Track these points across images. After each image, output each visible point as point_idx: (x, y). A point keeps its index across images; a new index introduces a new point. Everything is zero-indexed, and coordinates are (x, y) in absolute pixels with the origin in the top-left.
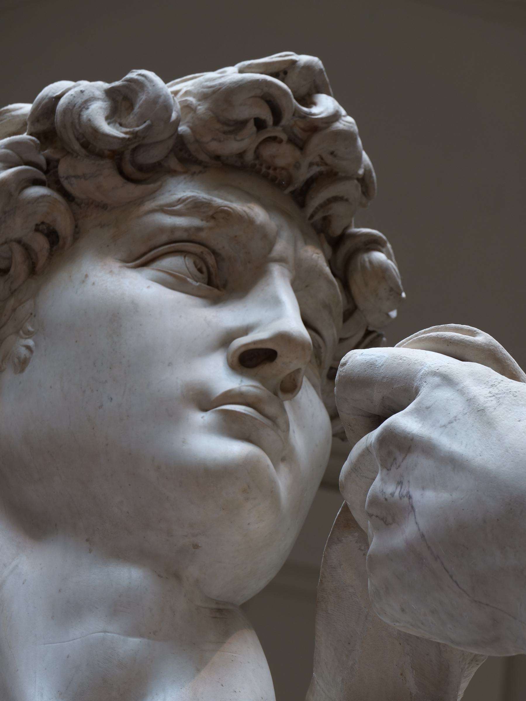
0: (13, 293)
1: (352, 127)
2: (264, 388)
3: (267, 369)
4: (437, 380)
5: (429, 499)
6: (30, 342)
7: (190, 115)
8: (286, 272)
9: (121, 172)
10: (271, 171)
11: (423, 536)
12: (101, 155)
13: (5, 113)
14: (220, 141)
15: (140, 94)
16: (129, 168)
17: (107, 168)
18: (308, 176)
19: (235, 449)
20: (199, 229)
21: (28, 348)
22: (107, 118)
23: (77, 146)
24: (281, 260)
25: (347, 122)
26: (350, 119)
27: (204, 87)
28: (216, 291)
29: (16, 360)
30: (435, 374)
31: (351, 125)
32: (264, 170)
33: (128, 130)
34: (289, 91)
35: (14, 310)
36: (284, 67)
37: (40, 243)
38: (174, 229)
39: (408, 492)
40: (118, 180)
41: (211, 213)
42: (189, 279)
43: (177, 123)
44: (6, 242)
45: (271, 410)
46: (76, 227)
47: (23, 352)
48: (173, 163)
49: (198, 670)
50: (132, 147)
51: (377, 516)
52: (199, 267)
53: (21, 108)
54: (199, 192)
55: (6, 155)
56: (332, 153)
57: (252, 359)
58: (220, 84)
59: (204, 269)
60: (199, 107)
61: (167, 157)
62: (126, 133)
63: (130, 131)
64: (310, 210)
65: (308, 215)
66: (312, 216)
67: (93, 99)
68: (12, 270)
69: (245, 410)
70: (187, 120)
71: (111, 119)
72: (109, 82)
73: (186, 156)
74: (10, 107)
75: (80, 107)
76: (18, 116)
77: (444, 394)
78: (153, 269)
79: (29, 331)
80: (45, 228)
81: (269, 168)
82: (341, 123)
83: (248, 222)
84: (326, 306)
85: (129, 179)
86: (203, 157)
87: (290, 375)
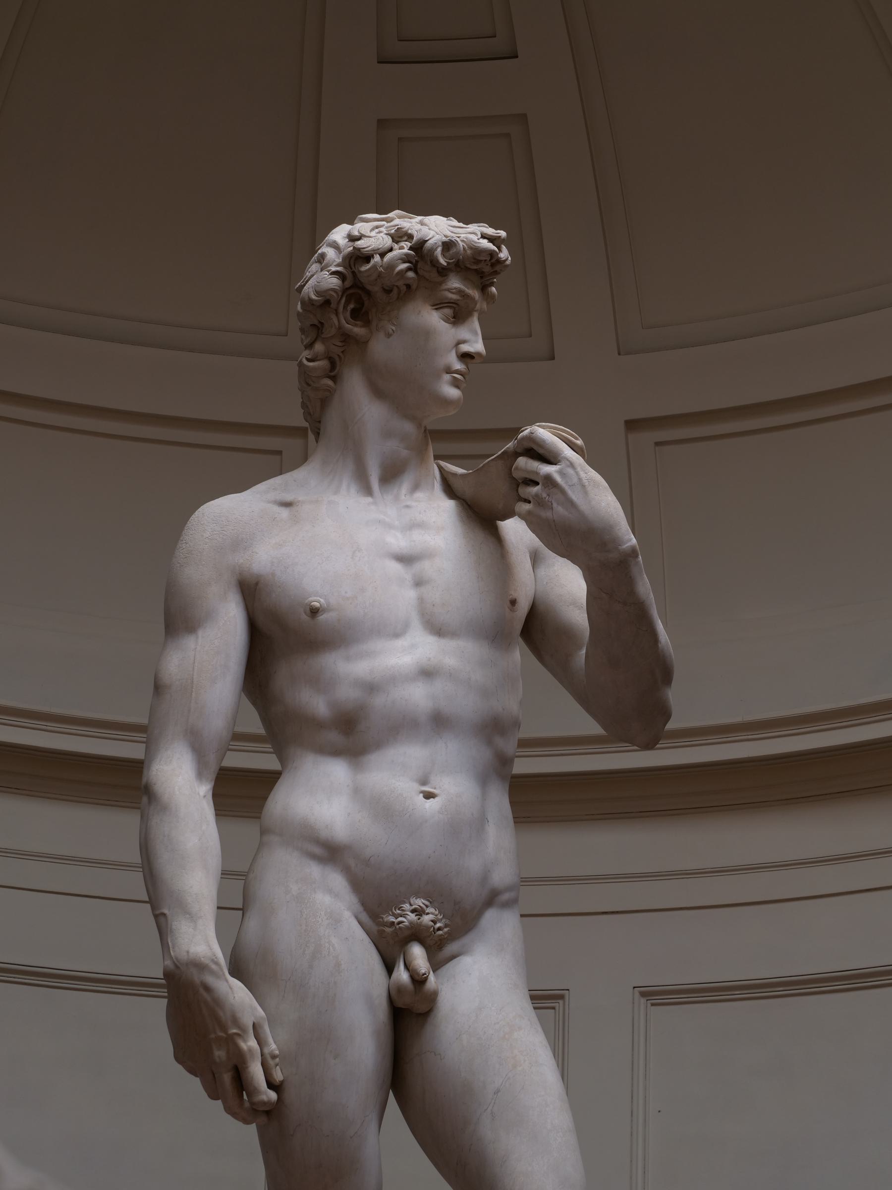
3: (469, 360)
5: (560, 510)
6: (394, 328)
9: (438, 272)
12: (434, 266)
37: (404, 288)
47: (391, 331)
77: (570, 471)
83: (472, 299)
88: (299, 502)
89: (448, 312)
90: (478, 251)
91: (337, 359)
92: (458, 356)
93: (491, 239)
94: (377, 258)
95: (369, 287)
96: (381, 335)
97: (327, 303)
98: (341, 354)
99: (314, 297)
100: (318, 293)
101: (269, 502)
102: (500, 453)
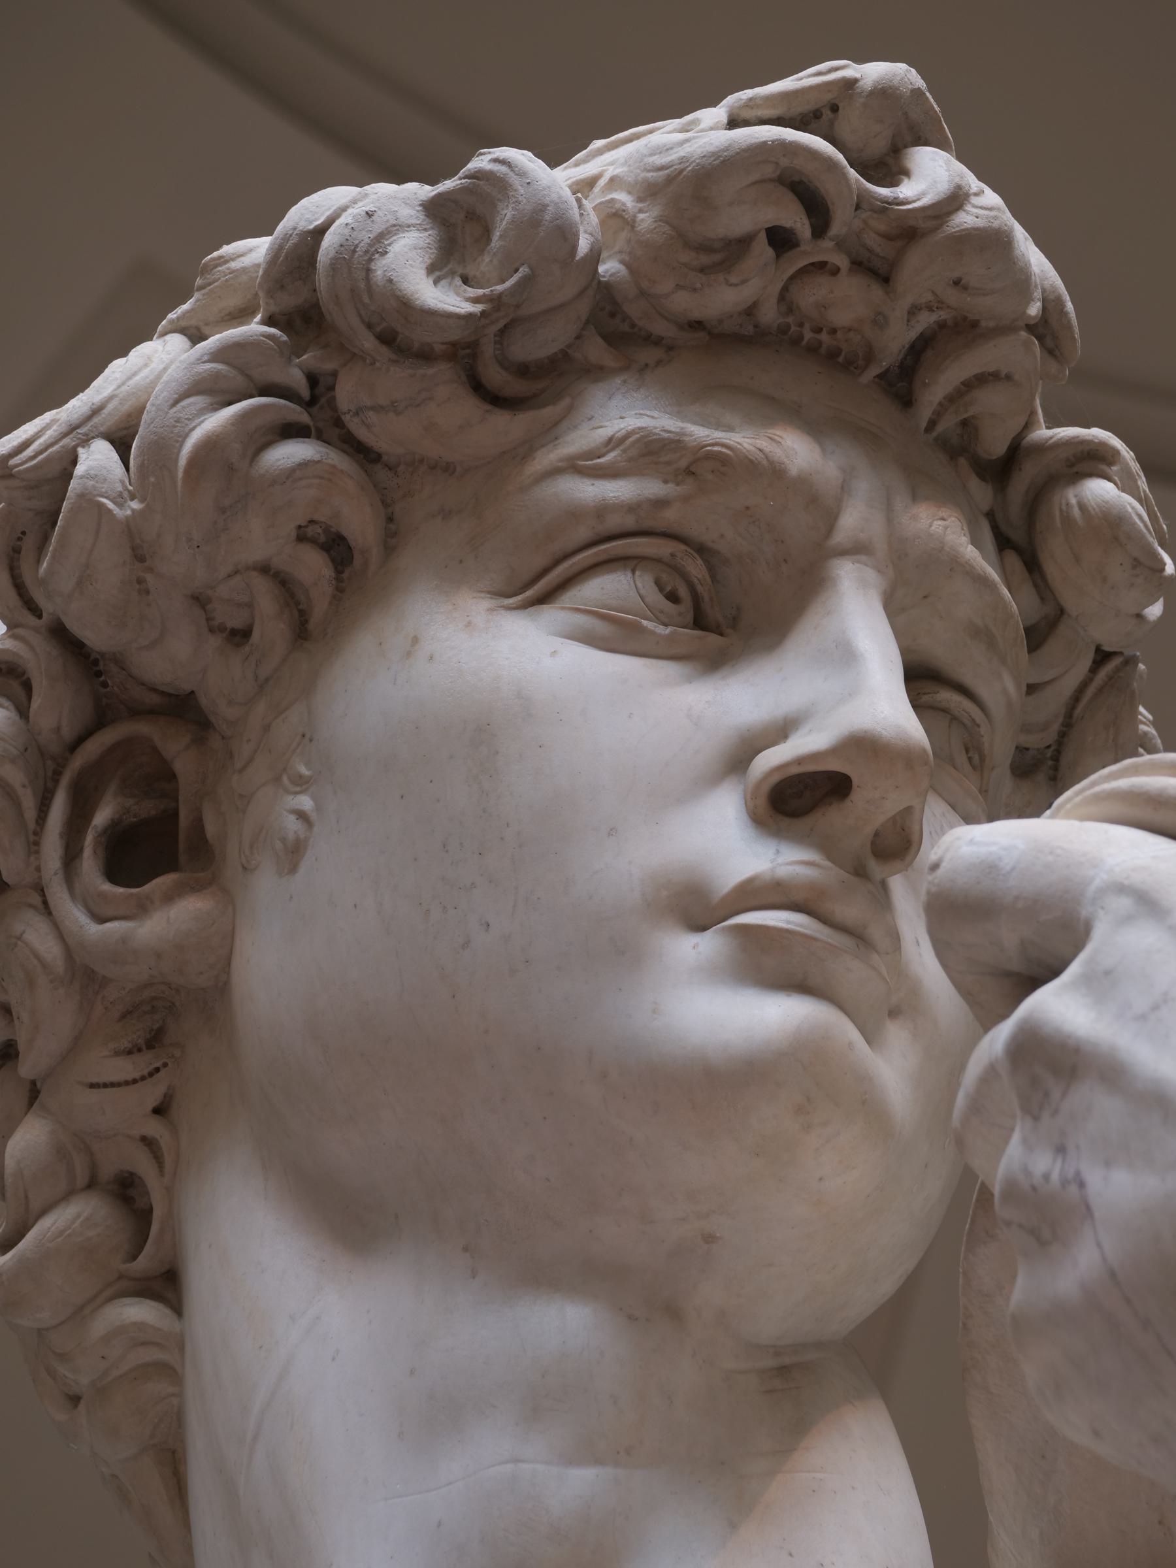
0: (262, 686)
1: (996, 218)
2: (828, 864)
3: (834, 818)
4: (1124, 904)
6: (305, 802)
7: (624, 235)
8: (871, 574)
9: (478, 387)
10: (824, 337)
11: (1112, 1274)
12: (425, 356)
13: (216, 266)
14: (695, 290)
15: (500, 206)
16: (494, 376)
17: (443, 379)
18: (913, 334)
19: (772, 1015)
20: (660, 503)
21: (302, 815)
22: (431, 269)
23: (368, 342)
24: (857, 550)
25: (986, 205)
26: (991, 198)
28: (713, 638)
29: (279, 845)
30: (1121, 889)
31: (993, 213)
32: (808, 335)
33: (480, 292)
34: (840, 157)
35: (267, 728)
36: (829, 97)
37: (312, 567)
38: (602, 510)
39: (1078, 1174)
40: (469, 406)
41: (683, 463)
42: (645, 622)
43: (594, 257)
44: (236, 572)
45: (850, 911)
46: (390, 519)
48: (595, 350)
49: (733, 1526)
50: (494, 328)
51: (1020, 1226)
52: (669, 588)
53: (251, 250)
54: (655, 414)
55: (216, 376)
56: (957, 283)
57: (797, 799)
58: (682, 160)
59: (683, 592)
60: (641, 216)
61: (578, 337)
62: (475, 300)
63: (484, 295)
64: (925, 413)
65: (924, 425)
66: (932, 424)
67: (395, 228)
69: (788, 922)
70: (617, 248)
71: (440, 269)
72: (432, 183)
73: (623, 332)
74: (226, 250)
75: (366, 252)
76: (244, 270)
78: (563, 608)
79: (301, 776)
80: (320, 531)
82: (968, 213)
83: (767, 472)
84: (982, 634)
85: (497, 400)
86: (660, 328)
87: (893, 819)
90: (688, 190)
91: (143, 1165)
94: (98, 457)
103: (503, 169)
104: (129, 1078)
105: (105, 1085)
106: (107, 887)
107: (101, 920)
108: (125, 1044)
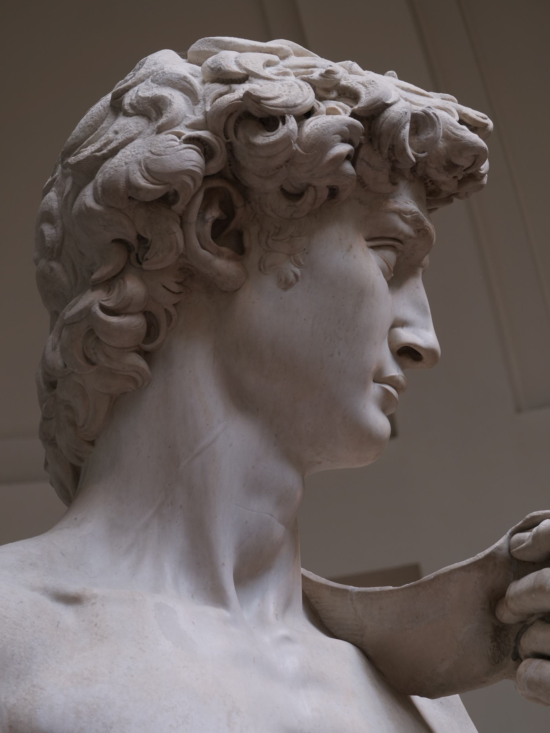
3: (408, 362)
6: (298, 271)
12: (389, 158)
15: (429, 129)
20: (411, 237)
21: (296, 275)
23: (386, 151)
27: (448, 128)
29: (283, 279)
32: (428, 181)
35: (292, 237)
38: (402, 232)
41: (420, 228)
47: (292, 277)
58: (462, 137)
60: (440, 142)
68: (299, 203)
79: (300, 263)
81: (430, 181)
88: (95, 596)
89: (390, 255)
90: (458, 145)
91: (163, 319)
92: (392, 350)
93: (475, 127)
94: (292, 123)
95: (252, 180)
96: (269, 283)
97: (167, 200)
98: (172, 310)
99: (142, 182)
100: (150, 173)
101: (34, 589)
102: (481, 555)
103: (436, 119)
104: (172, 290)
105: (167, 289)
106: (211, 240)
107: (204, 248)
108: (179, 281)
